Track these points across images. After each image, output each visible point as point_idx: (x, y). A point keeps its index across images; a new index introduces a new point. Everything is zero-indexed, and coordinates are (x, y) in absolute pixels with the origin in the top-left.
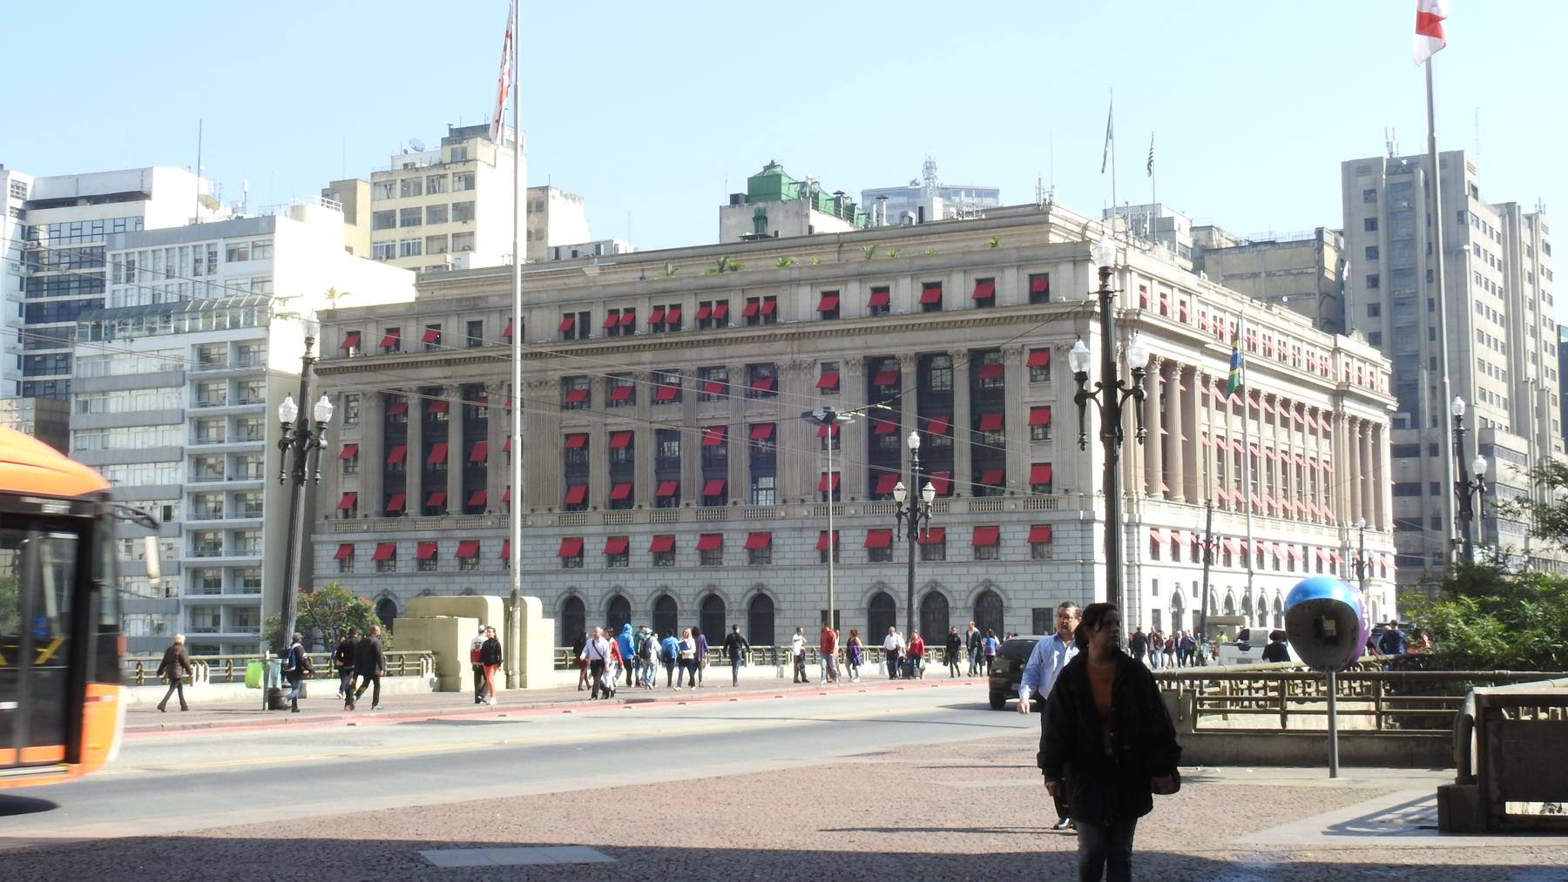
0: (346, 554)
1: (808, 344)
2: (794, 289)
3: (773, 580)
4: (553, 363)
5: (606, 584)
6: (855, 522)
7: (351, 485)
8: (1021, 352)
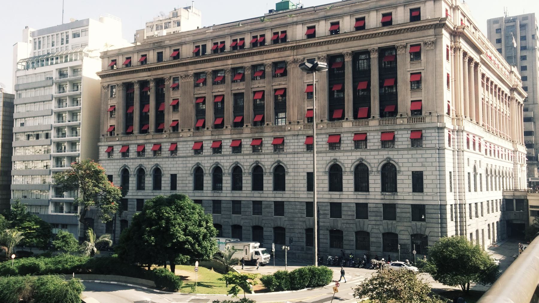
0: (110, 151)
1: (301, 51)
2: (295, 27)
3: (285, 159)
4: (191, 67)
5: (212, 161)
6: (323, 131)
7: (113, 122)
8: (405, 47)
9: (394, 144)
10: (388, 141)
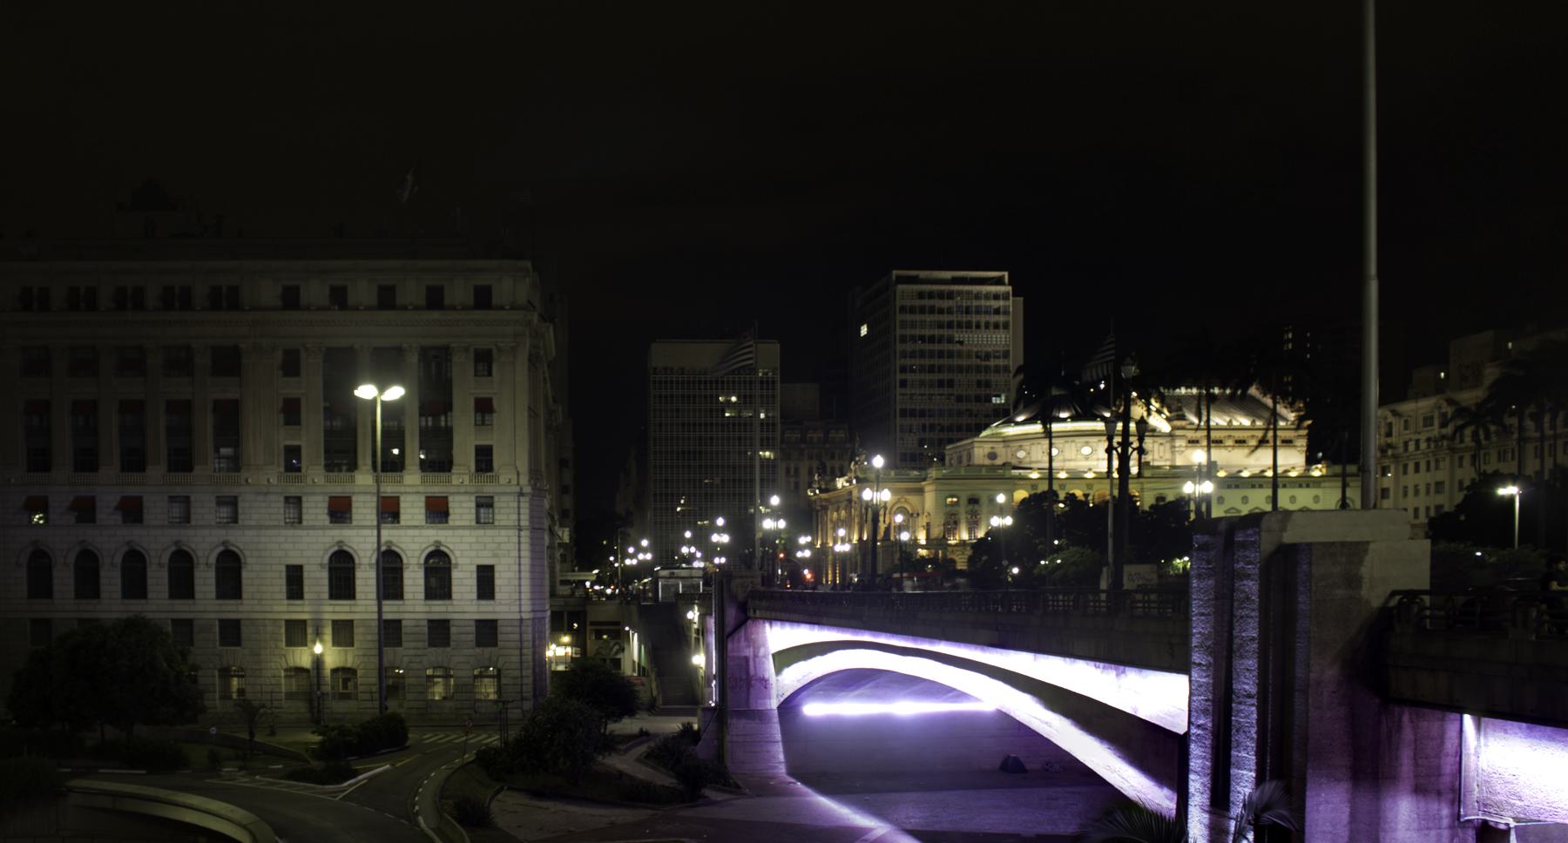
3: (239, 539)
10: (438, 511)
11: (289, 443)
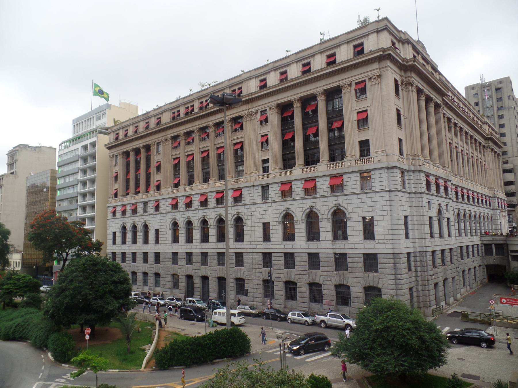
1: (255, 104)
2: (249, 81)
3: (243, 211)
8: (350, 85)
9: (342, 189)
10: (337, 186)
11: (263, 158)
